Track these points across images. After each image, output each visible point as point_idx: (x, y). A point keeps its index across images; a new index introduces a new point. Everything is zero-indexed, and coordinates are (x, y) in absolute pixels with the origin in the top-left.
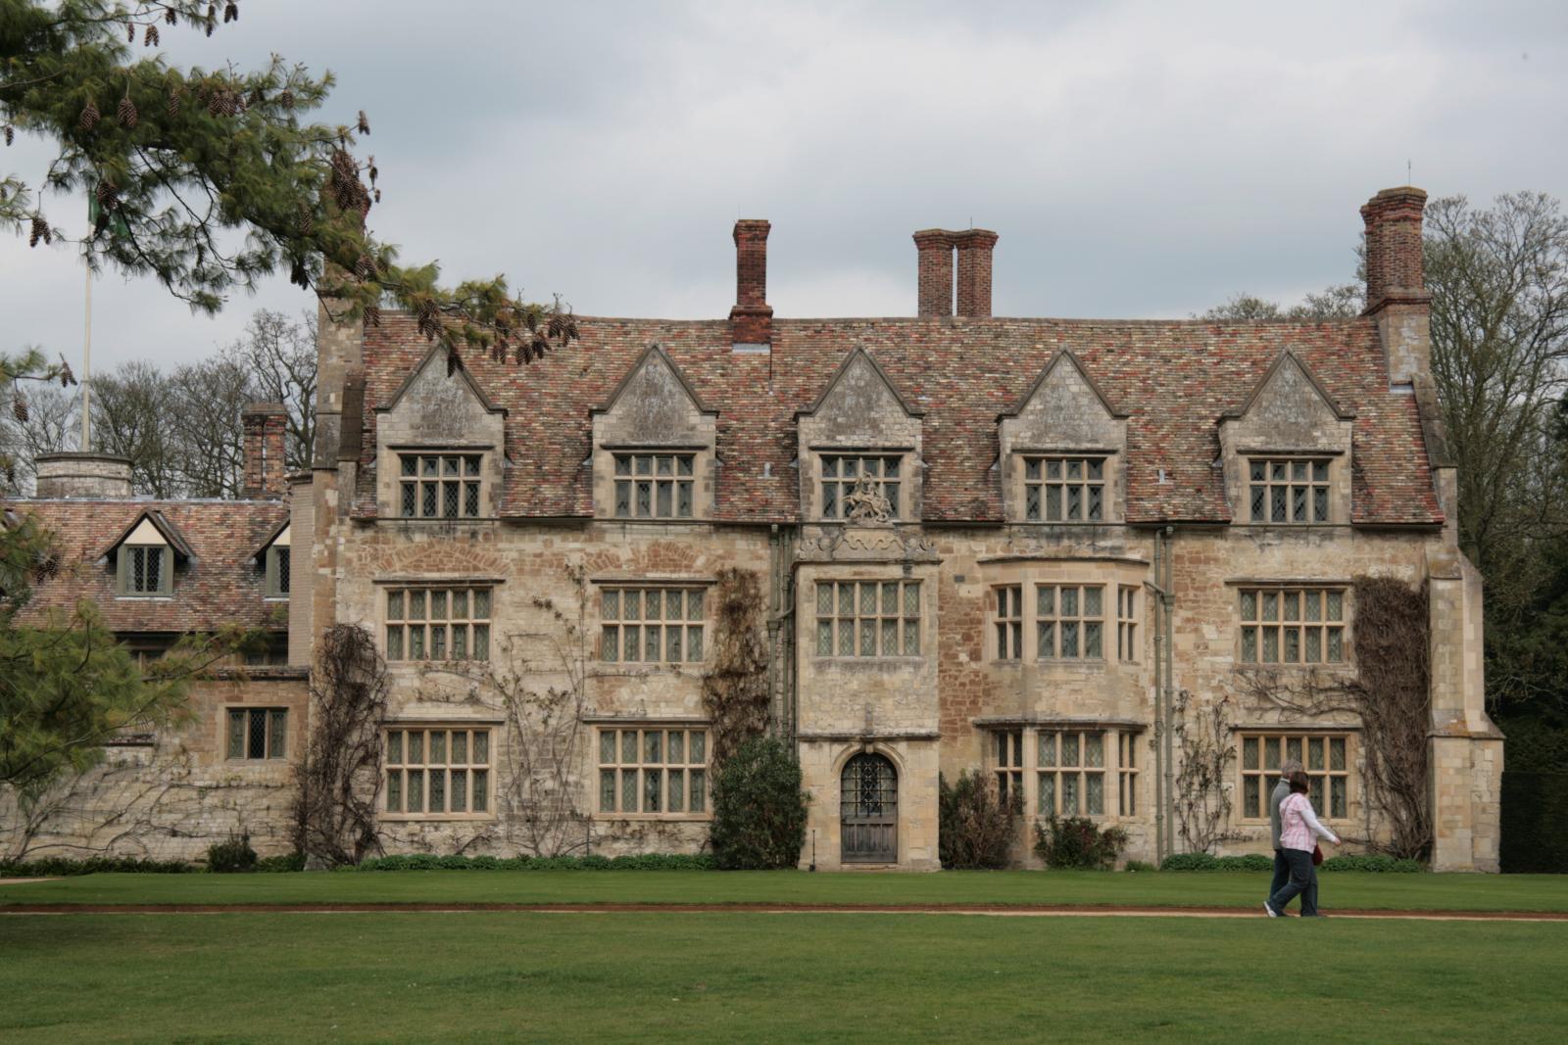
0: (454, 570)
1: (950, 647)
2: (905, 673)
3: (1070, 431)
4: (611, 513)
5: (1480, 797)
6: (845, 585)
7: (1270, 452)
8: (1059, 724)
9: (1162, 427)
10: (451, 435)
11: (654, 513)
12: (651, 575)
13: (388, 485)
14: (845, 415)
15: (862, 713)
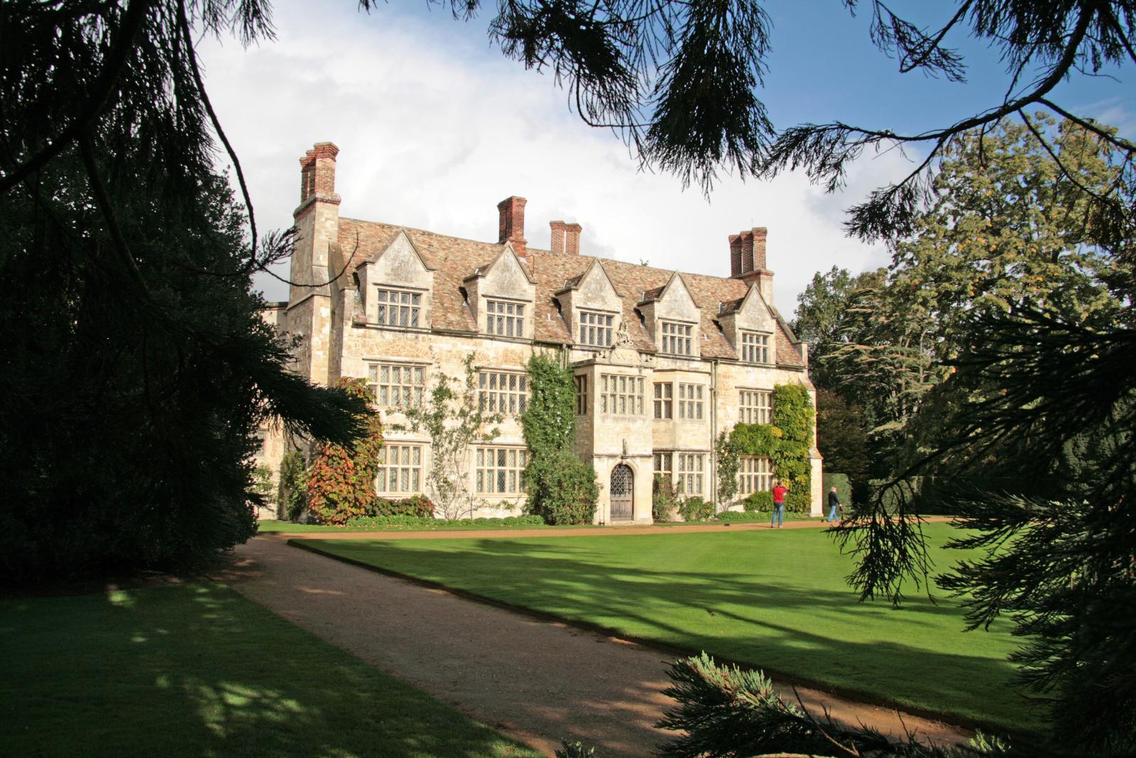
2: (639, 423)
4: (485, 332)
6: (614, 377)
11: (505, 333)
12: (504, 366)
13: (372, 306)
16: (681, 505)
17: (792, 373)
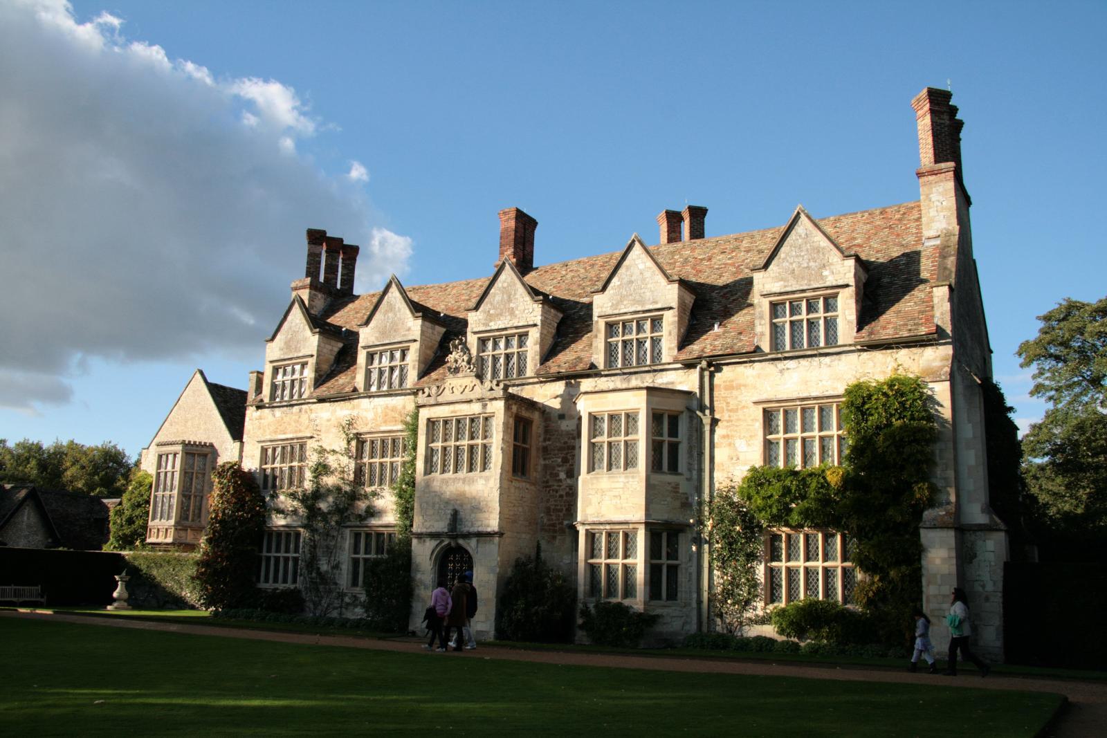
0: (290, 433)
1: (553, 468)
3: (638, 298)
5: (983, 586)
7: (787, 293)
8: (601, 524)
9: (736, 294)
10: (296, 351)
14: (494, 308)
15: (449, 516)
16: (585, 613)
17: (903, 354)
